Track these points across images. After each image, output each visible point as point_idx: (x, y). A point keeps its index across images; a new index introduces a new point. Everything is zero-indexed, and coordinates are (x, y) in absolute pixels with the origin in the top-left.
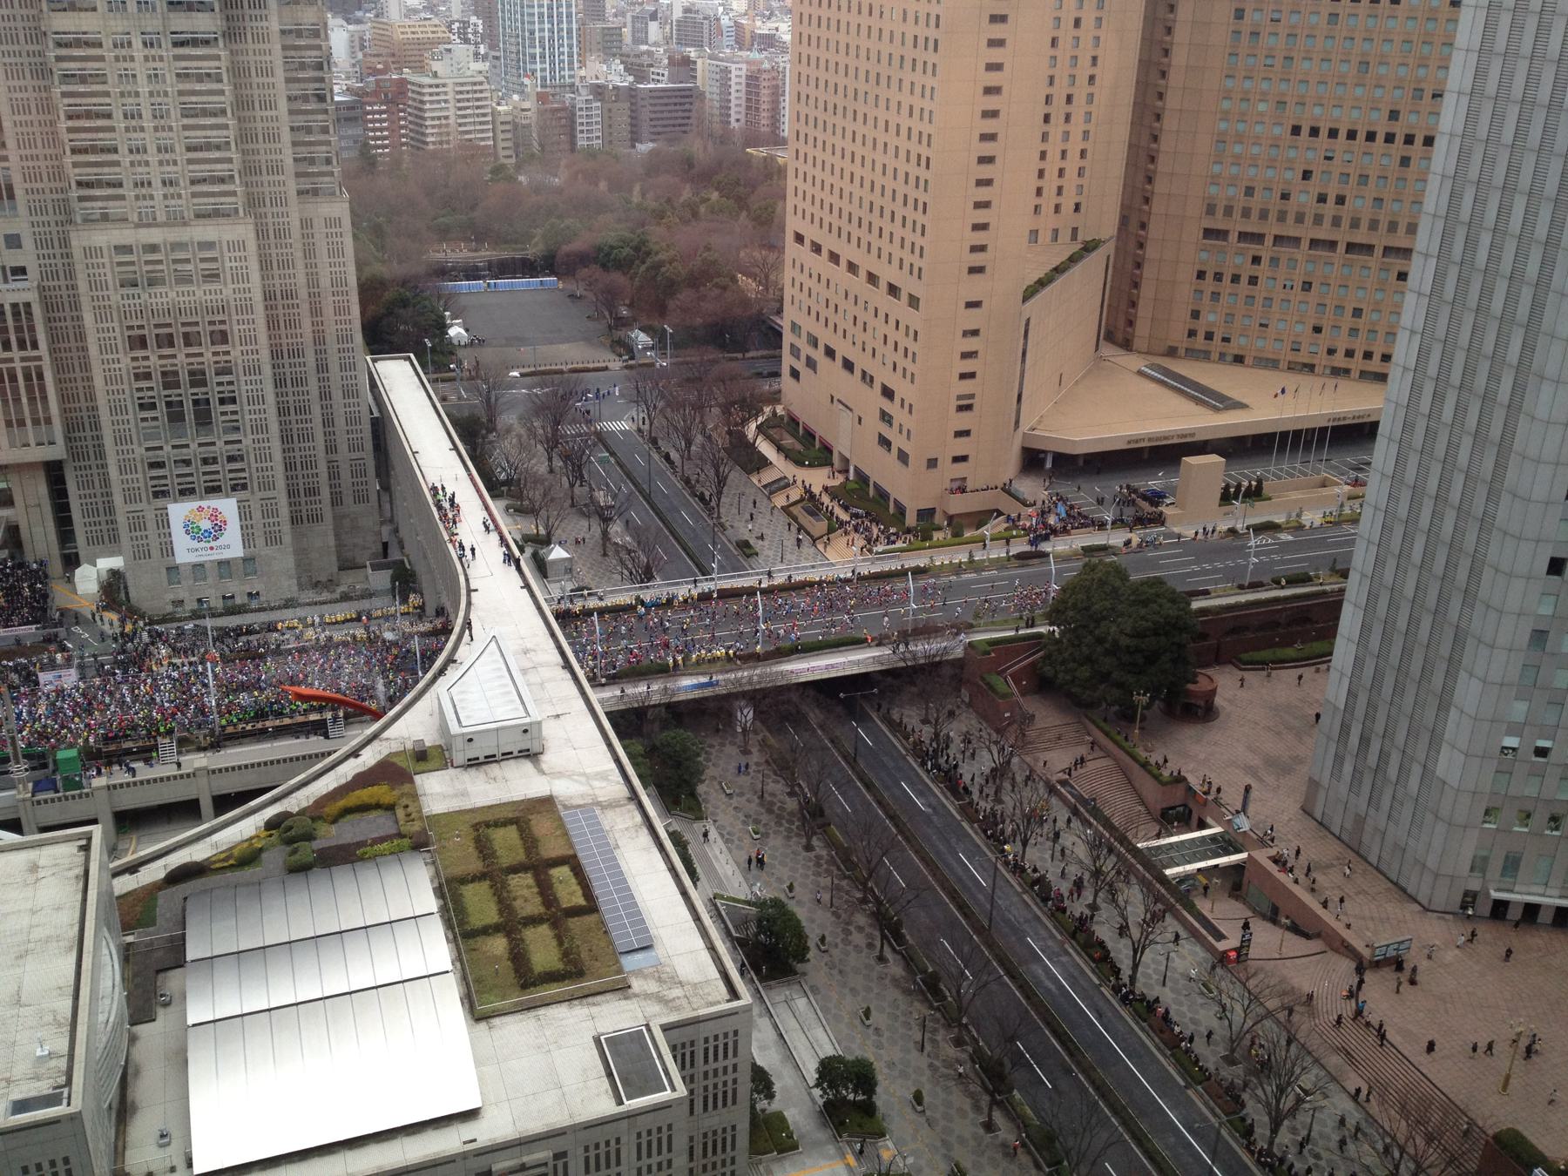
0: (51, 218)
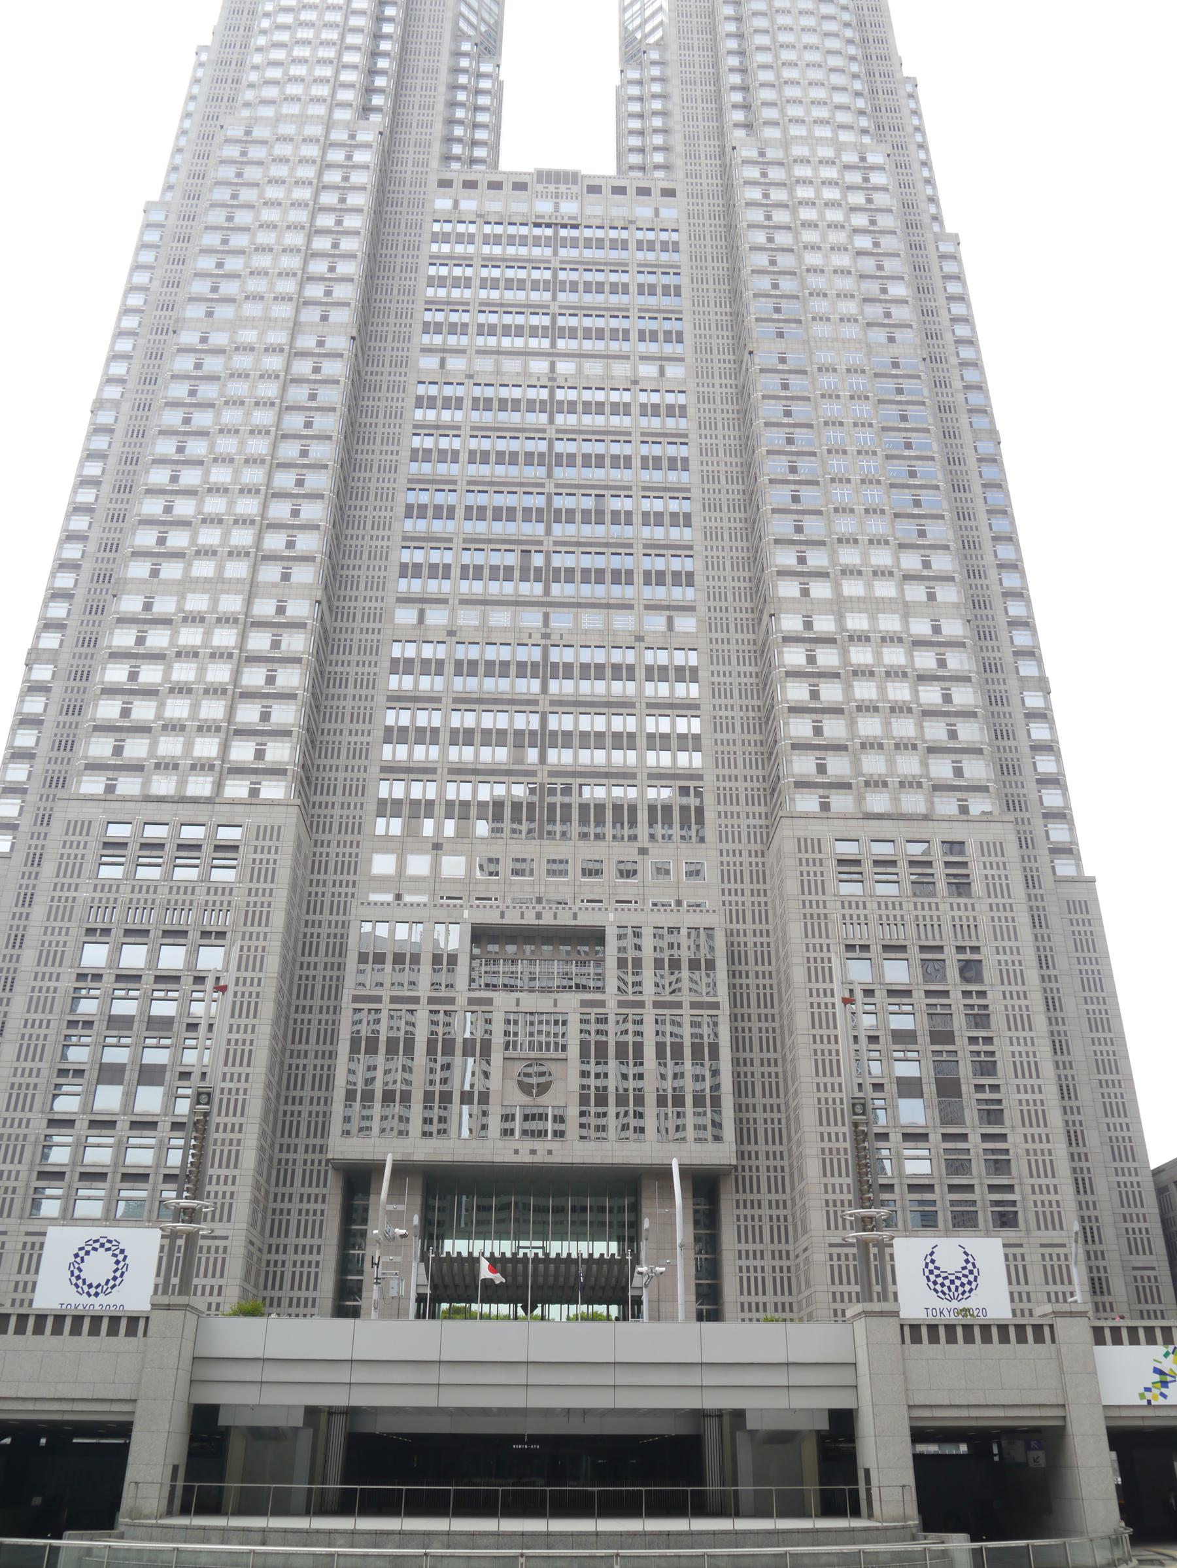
0: (744, 846)
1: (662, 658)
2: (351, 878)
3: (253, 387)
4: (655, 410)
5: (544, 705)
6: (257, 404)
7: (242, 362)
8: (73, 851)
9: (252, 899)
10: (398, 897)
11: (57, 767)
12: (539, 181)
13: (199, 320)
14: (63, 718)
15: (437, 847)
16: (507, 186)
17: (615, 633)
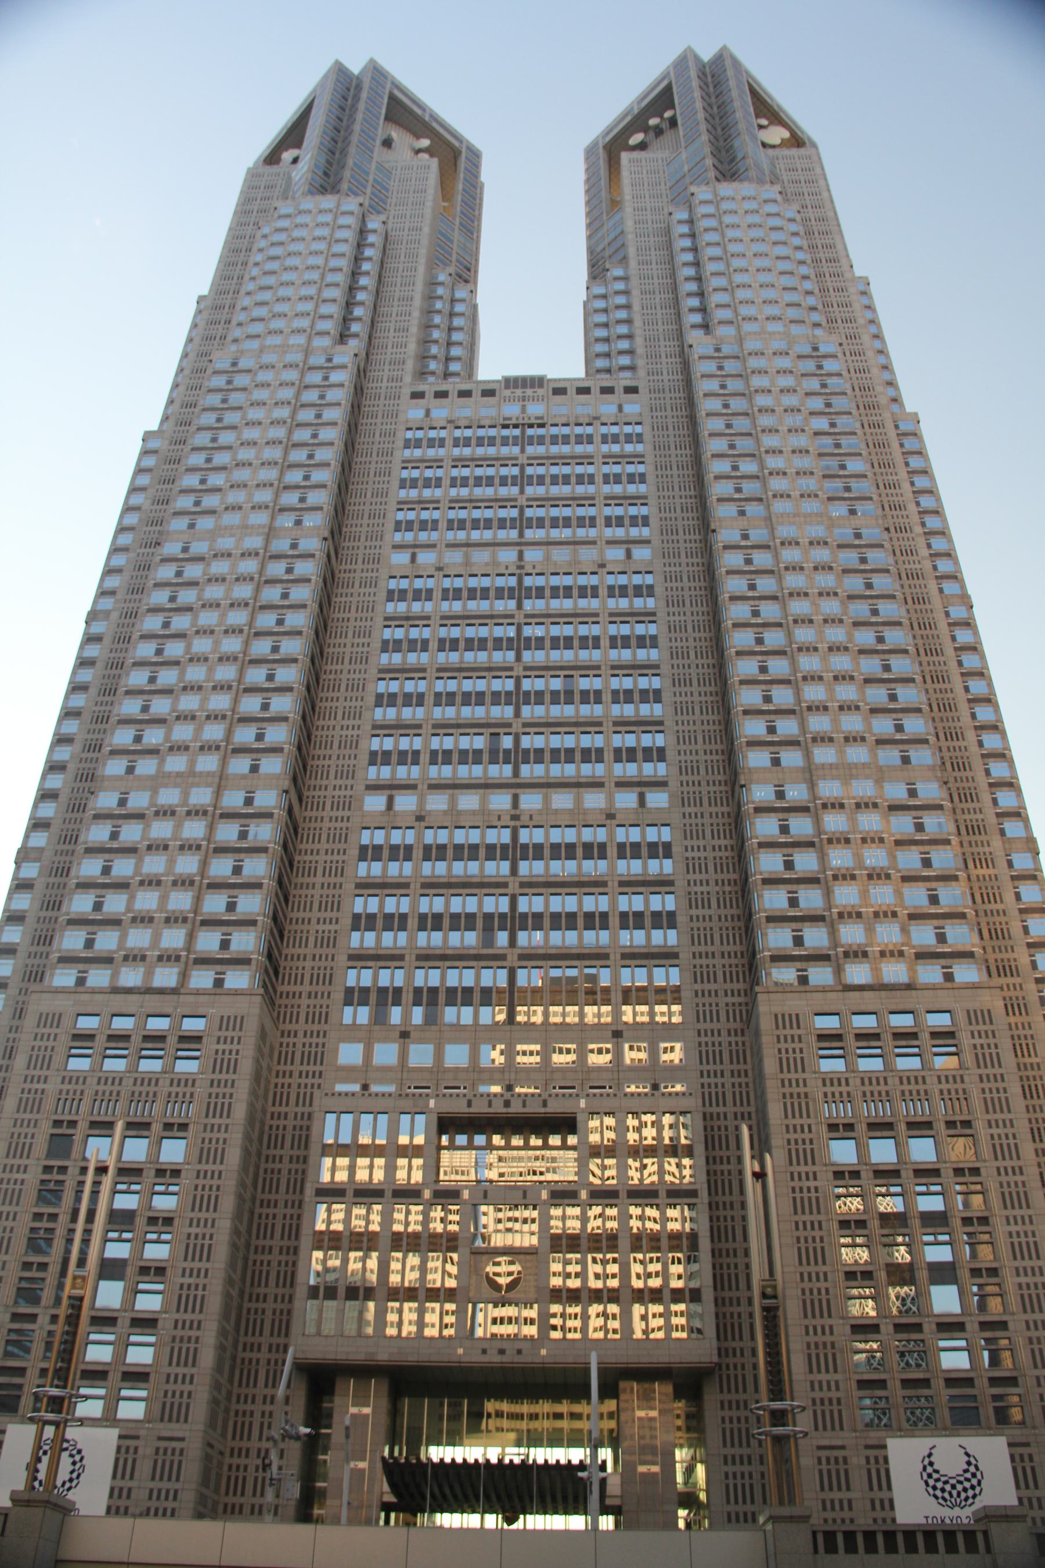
0: (723, 1025)
1: (634, 835)
2: (318, 1068)
3: (229, 590)
4: (623, 591)
5: (513, 887)
6: (232, 605)
7: (220, 567)
8: (44, 1043)
9: (215, 1090)
10: (365, 1087)
11: (37, 961)
12: (507, 387)
13: (182, 532)
14: (43, 914)
15: (405, 1035)
16: (477, 393)
17: (586, 812)
